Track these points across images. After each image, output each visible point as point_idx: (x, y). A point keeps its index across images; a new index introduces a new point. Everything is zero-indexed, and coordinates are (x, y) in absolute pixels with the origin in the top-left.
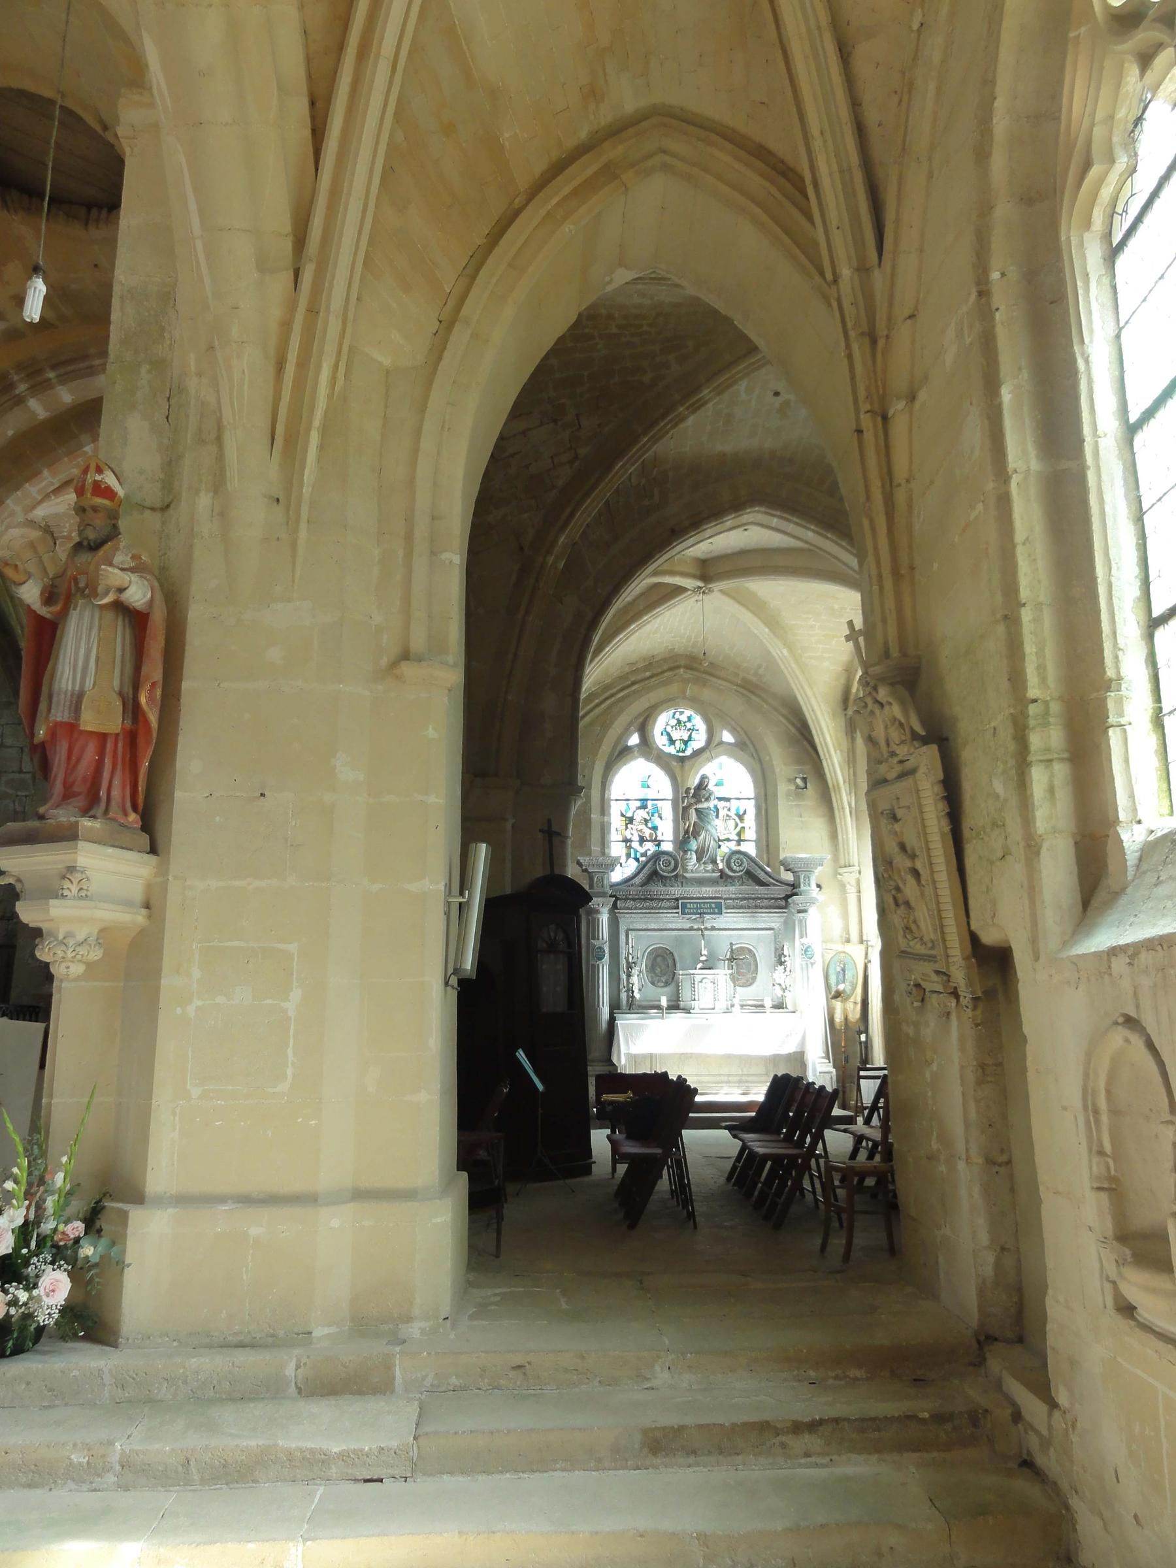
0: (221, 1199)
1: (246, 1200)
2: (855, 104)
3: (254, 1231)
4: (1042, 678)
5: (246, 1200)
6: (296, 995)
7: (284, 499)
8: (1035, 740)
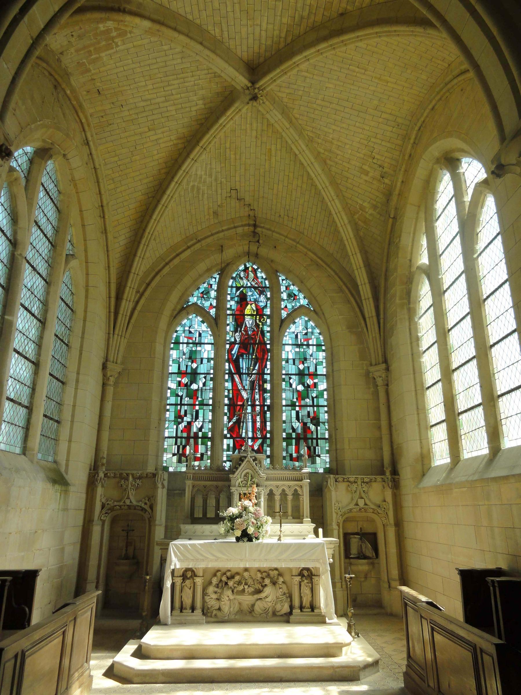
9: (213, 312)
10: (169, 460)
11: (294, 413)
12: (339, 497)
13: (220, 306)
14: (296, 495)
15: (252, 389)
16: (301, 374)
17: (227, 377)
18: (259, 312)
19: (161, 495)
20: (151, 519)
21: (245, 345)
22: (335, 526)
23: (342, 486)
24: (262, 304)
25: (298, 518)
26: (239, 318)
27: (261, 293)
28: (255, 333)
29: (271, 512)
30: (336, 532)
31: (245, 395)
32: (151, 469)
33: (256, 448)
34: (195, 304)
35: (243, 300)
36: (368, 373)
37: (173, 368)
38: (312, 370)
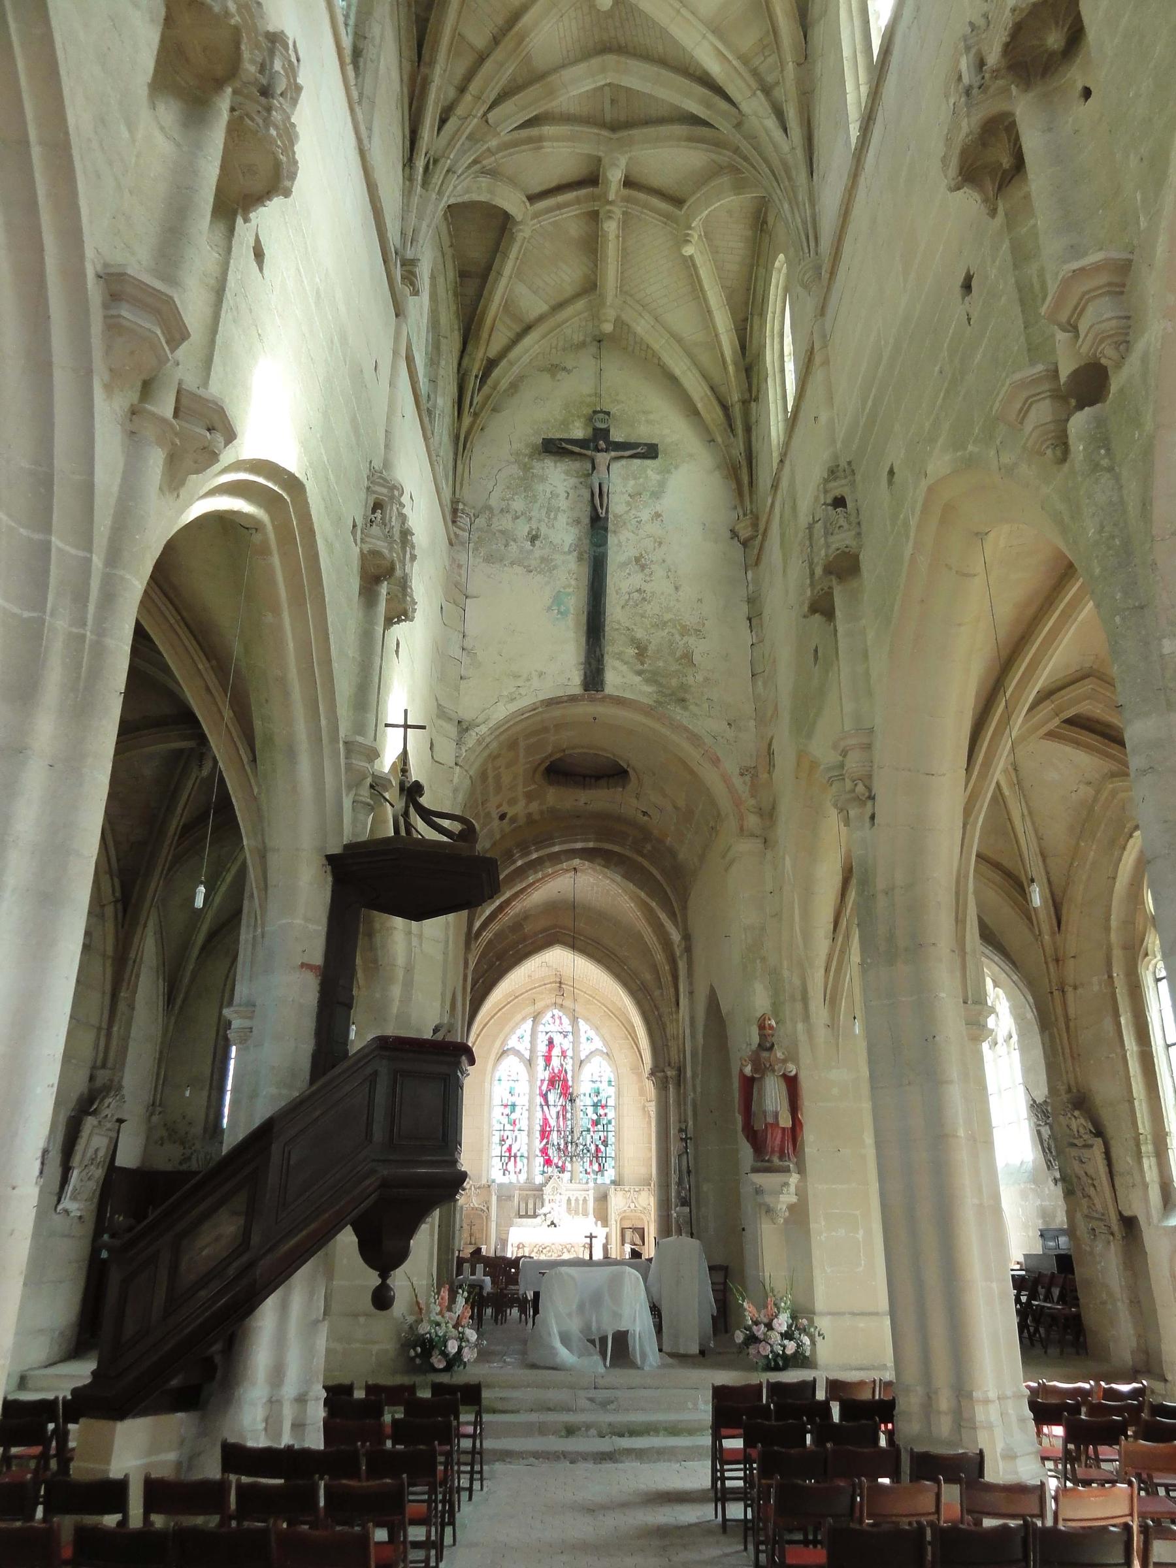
0: (843, 1314)
1: (854, 1314)
2: (1047, 873)
3: (861, 1325)
4: (1144, 1126)
5: (854, 1314)
6: (861, 1232)
7: (832, 1026)
8: (1143, 1149)
9: (527, 1055)
10: (497, 1175)
11: (589, 1137)
12: (618, 1202)
13: (532, 1050)
14: (585, 1200)
15: (558, 1118)
16: (595, 1105)
17: (539, 1108)
18: (564, 1054)
19: (494, 1198)
20: (488, 1218)
21: (552, 1082)
22: (613, 1222)
23: (620, 1194)
24: (565, 1048)
25: (586, 1214)
26: (548, 1059)
27: (565, 1036)
28: (560, 1072)
29: (569, 1210)
30: (614, 1227)
31: (553, 1122)
32: (484, 1182)
33: (560, 1164)
34: (513, 1048)
35: (551, 1043)
36: (644, 1107)
37: (496, 1101)
38: (603, 1102)
